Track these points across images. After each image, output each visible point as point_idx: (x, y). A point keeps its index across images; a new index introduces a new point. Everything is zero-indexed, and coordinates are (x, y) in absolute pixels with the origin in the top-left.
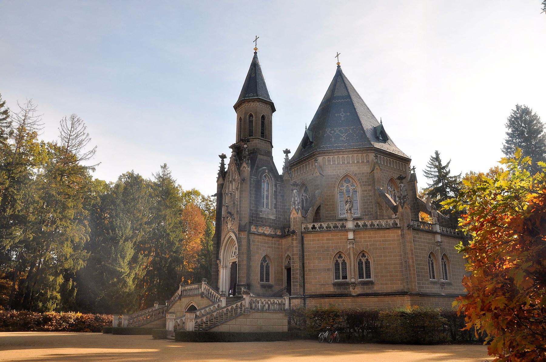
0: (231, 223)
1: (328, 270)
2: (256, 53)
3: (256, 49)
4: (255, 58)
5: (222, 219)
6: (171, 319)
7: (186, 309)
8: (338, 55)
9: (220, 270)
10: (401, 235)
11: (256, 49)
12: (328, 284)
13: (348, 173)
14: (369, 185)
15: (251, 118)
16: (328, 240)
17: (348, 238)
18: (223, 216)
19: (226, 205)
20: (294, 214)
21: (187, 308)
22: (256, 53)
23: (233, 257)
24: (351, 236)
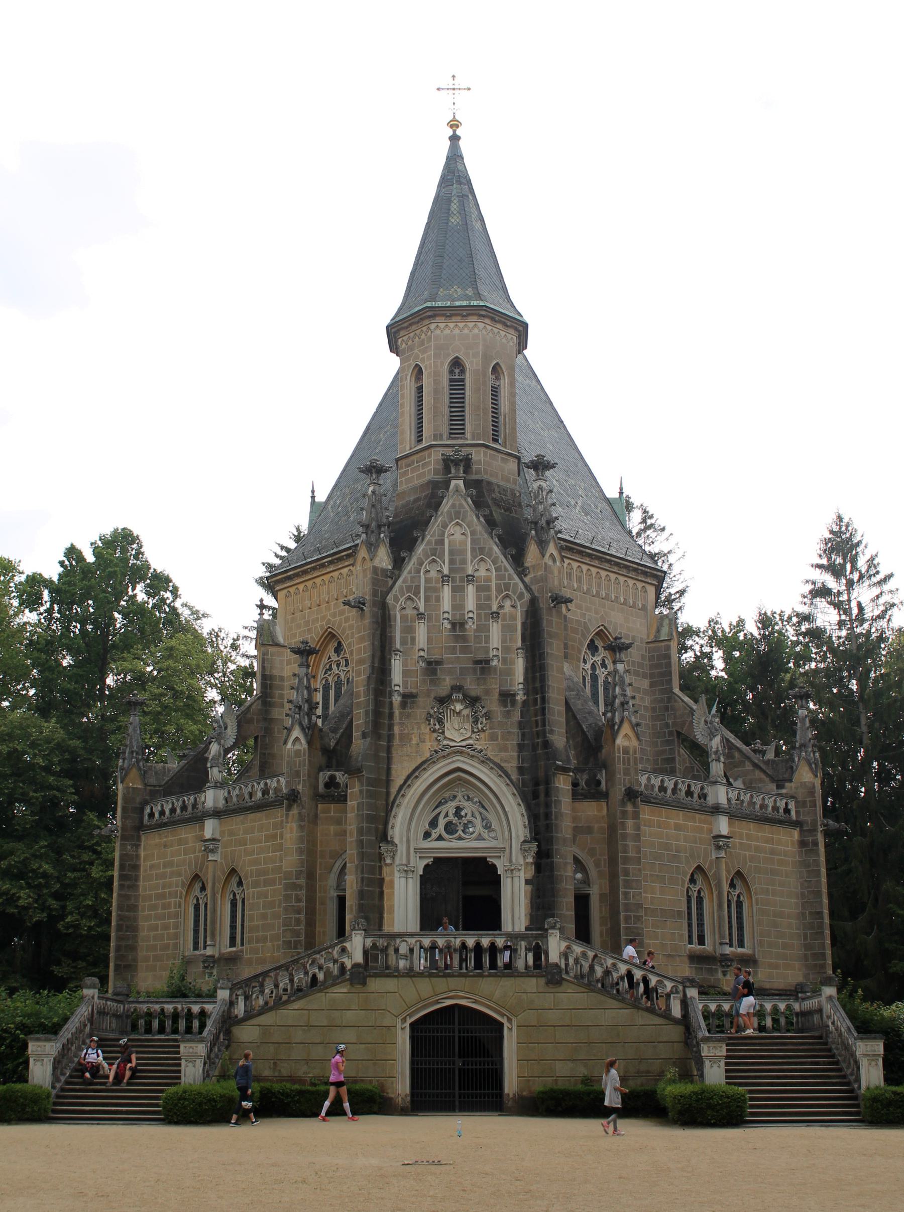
0: (468, 726)
1: (679, 912)
2: (455, 139)
3: (454, 124)
4: (454, 159)
5: (397, 699)
6: (714, 1059)
7: (404, 1020)
9: (387, 879)
10: (802, 844)
11: (454, 124)
12: (679, 956)
13: (605, 628)
14: (644, 676)
16: (678, 827)
17: (711, 831)
18: (397, 688)
19: (422, 653)
20: (626, 735)
21: (410, 1015)
22: (455, 139)
23: (440, 838)
24: (723, 826)
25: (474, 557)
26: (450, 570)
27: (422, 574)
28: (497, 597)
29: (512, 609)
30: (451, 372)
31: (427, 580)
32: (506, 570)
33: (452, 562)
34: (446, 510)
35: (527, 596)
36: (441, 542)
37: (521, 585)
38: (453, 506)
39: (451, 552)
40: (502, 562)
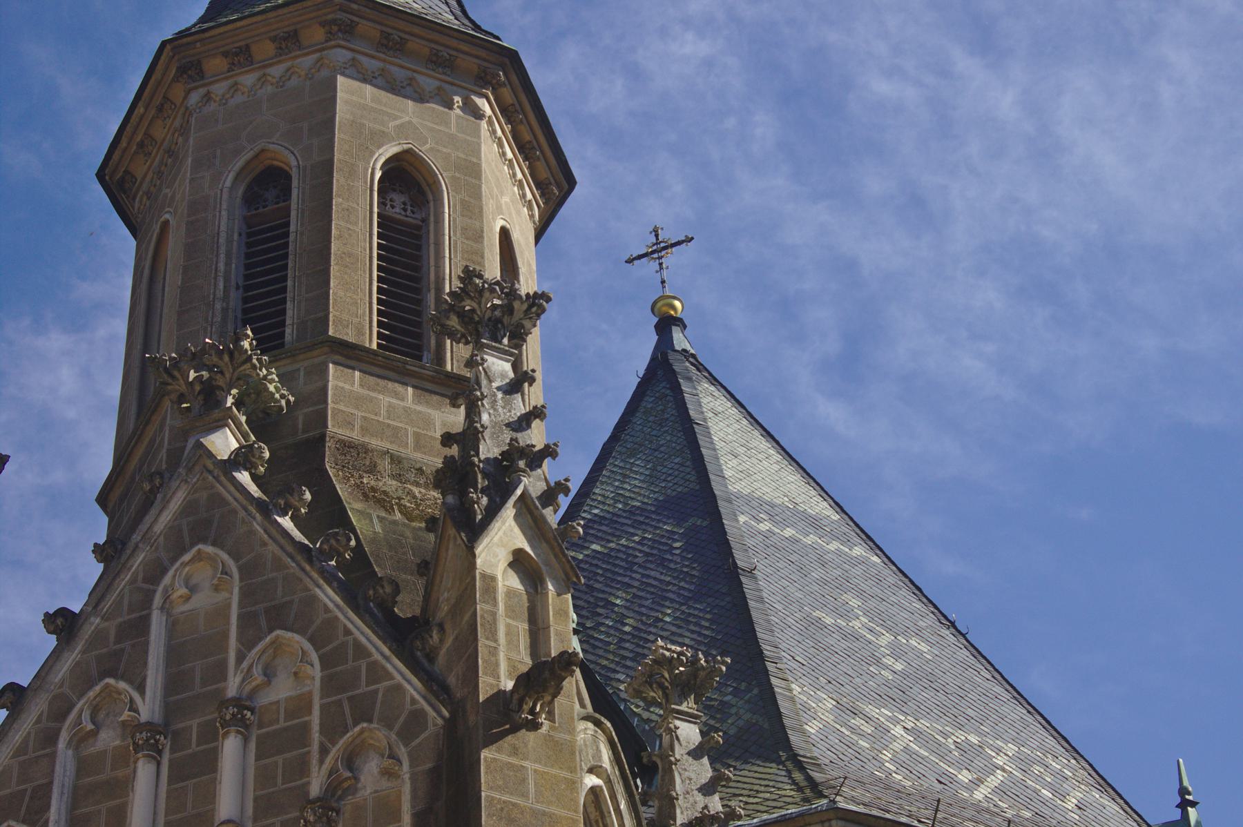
8: (659, 249)
15: (398, 199)
25: (247, 643)
26: (172, 710)
27: (61, 744)
28: (324, 751)
29: (385, 783)
30: (251, 199)
31: (84, 766)
32: (361, 651)
33: (174, 683)
34: (159, 528)
35: (435, 717)
36: (140, 627)
37: (413, 688)
38: (189, 508)
39: (174, 654)
40: (348, 632)
